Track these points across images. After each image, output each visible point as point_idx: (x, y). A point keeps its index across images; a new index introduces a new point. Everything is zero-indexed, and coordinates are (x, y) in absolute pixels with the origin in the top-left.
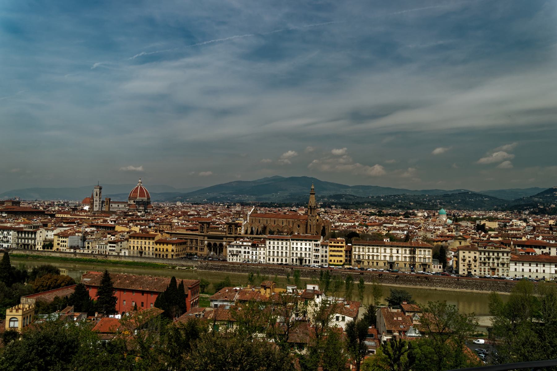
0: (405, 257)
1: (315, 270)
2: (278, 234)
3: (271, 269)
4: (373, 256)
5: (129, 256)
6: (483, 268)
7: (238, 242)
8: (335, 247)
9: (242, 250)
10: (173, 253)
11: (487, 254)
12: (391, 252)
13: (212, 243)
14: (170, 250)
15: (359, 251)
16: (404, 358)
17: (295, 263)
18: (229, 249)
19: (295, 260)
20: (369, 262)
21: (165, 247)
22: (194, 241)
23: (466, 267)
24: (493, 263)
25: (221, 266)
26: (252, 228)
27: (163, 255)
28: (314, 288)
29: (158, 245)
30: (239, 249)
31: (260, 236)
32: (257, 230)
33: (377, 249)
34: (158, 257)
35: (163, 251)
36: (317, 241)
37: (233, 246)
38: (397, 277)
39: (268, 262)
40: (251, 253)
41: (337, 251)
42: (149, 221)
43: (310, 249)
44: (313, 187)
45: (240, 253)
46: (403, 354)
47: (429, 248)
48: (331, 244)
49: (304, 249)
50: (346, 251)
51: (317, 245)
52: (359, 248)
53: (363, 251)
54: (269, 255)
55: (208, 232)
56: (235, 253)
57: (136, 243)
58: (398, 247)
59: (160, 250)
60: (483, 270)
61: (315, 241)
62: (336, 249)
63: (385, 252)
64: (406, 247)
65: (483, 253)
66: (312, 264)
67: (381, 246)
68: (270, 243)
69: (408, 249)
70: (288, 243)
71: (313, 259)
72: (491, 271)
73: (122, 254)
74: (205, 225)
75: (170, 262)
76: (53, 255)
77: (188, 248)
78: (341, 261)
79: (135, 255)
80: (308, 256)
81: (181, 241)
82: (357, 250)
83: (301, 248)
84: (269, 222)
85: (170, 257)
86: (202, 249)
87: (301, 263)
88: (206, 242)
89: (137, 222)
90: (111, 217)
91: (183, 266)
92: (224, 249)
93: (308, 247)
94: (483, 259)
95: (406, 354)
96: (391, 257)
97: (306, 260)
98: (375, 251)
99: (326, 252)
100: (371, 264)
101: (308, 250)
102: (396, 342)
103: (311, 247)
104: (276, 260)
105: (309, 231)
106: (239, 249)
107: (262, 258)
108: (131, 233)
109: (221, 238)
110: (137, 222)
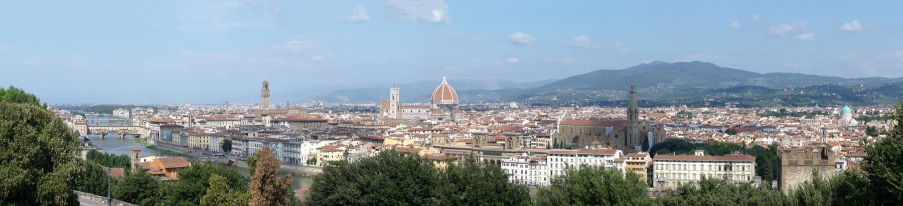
8: (633, 163)
13: (489, 160)
63: (695, 169)
82: (660, 167)
88: (482, 159)
89: (422, 133)
90: (398, 127)
106: (515, 168)
109: (499, 153)
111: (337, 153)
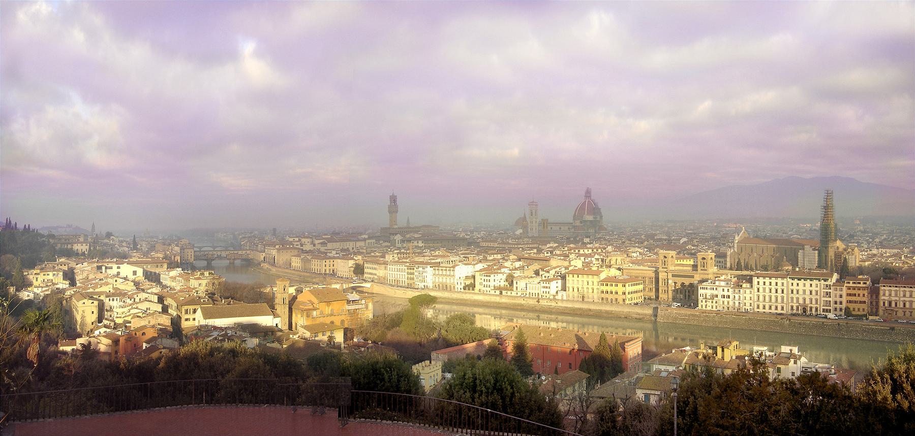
5: (567, 301)
14: (620, 293)
15: (890, 295)
19: (795, 308)
21: (614, 289)
25: (689, 315)
30: (715, 292)
39: (756, 310)
49: (808, 292)
53: (896, 295)
57: (576, 282)
73: (559, 297)
76: (476, 297)
79: (576, 299)
82: (887, 293)
90: (548, 246)
93: (814, 288)
97: (811, 308)
99: (841, 296)
103: (818, 289)
108: (570, 269)
110: (581, 252)
111: (500, 276)
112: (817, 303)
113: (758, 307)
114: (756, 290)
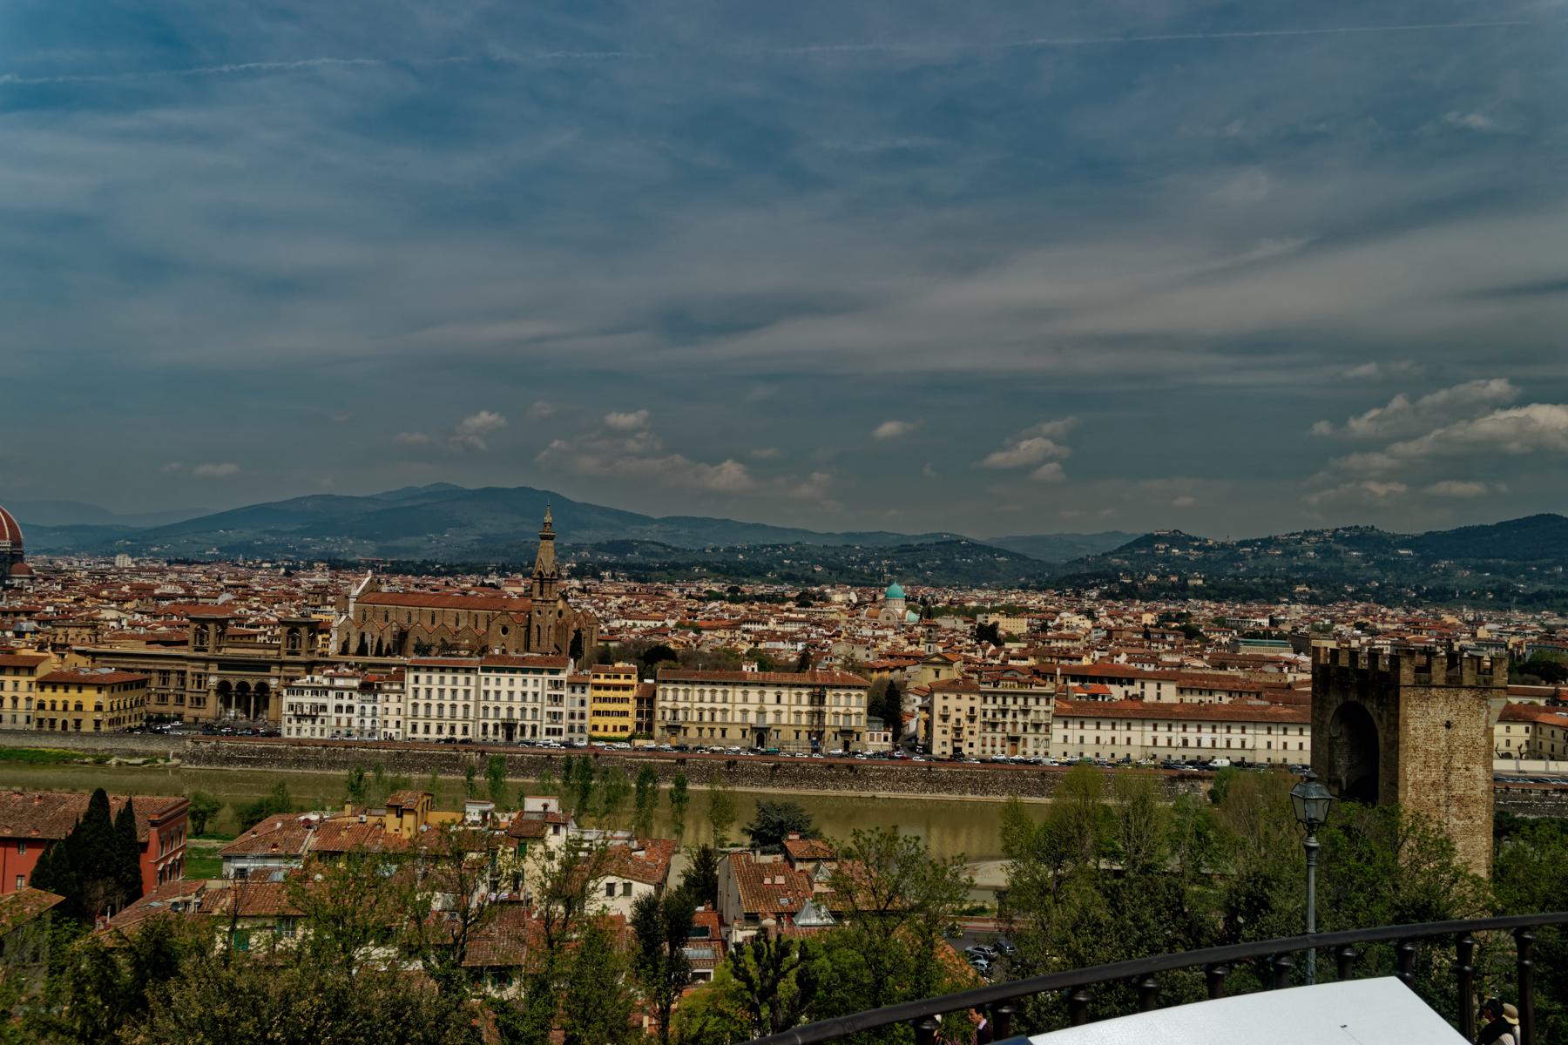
0: (798, 713)
1: (549, 756)
2: (443, 654)
3: (419, 755)
4: (713, 711)
6: (989, 736)
7: (317, 678)
8: (607, 687)
9: (331, 701)
10: (98, 716)
11: (999, 700)
12: (762, 700)
13: (234, 682)
14: (89, 706)
16: (787, 987)
17: (491, 736)
18: (288, 699)
19: (491, 729)
20: (700, 730)
21: (73, 696)
22: (174, 676)
23: (951, 735)
24: (1014, 724)
25: (261, 751)
26: (363, 635)
27: (65, 723)
28: (545, 806)
29: (48, 691)
30: (320, 700)
31: (388, 660)
32: (380, 643)
33: (725, 692)
34: (46, 728)
35: (65, 708)
36: (556, 672)
37: (301, 691)
38: (774, 768)
39: (410, 735)
40: (357, 709)
41: (614, 700)
42: (17, 613)
43: (535, 694)
44: (548, 519)
45: (322, 711)
46: (784, 975)
47: (859, 688)
48: (596, 681)
49: (517, 696)
50: (640, 700)
51: (556, 685)
52: (676, 690)
53: (686, 698)
54: (415, 716)
55: (219, 649)
56: (307, 711)
58: (779, 685)
59: (53, 708)
60: (989, 742)
61: (552, 672)
62: (611, 694)
63: (745, 700)
64: (799, 686)
65: (990, 700)
66: (542, 738)
67: (734, 685)
68: (417, 679)
69: (805, 691)
70: (473, 678)
71: (545, 723)
72: (1008, 744)
74: (211, 626)
75: (88, 744)
77: (153, 698)
78: (624, 728)
80: (529, 714)
81: (127, 677)
82: (670, 695)
83: (511, 693)
84: (415, 619)
85: (88, 727)
86: (199, 702)
87: (510, 737)
88: (213, 680)
91: (134, 754)
92: (272, 702)
93: (530, 688)
94: (990, 714)
95: (793, 974)
96: (761, 713)
97: (523, 728)
98: (719, 696)
99: (583, 703)
100: (706, 733)
101: (530, 697)
102: (768, 942)
103: (538, 689)
104: (433, 728)
105: (533, 644)
106: (320, 700)
107: (392, 724)
109: (264, 666)
112: (534, 717)
113: (414, 727)
114: (411, 693)
